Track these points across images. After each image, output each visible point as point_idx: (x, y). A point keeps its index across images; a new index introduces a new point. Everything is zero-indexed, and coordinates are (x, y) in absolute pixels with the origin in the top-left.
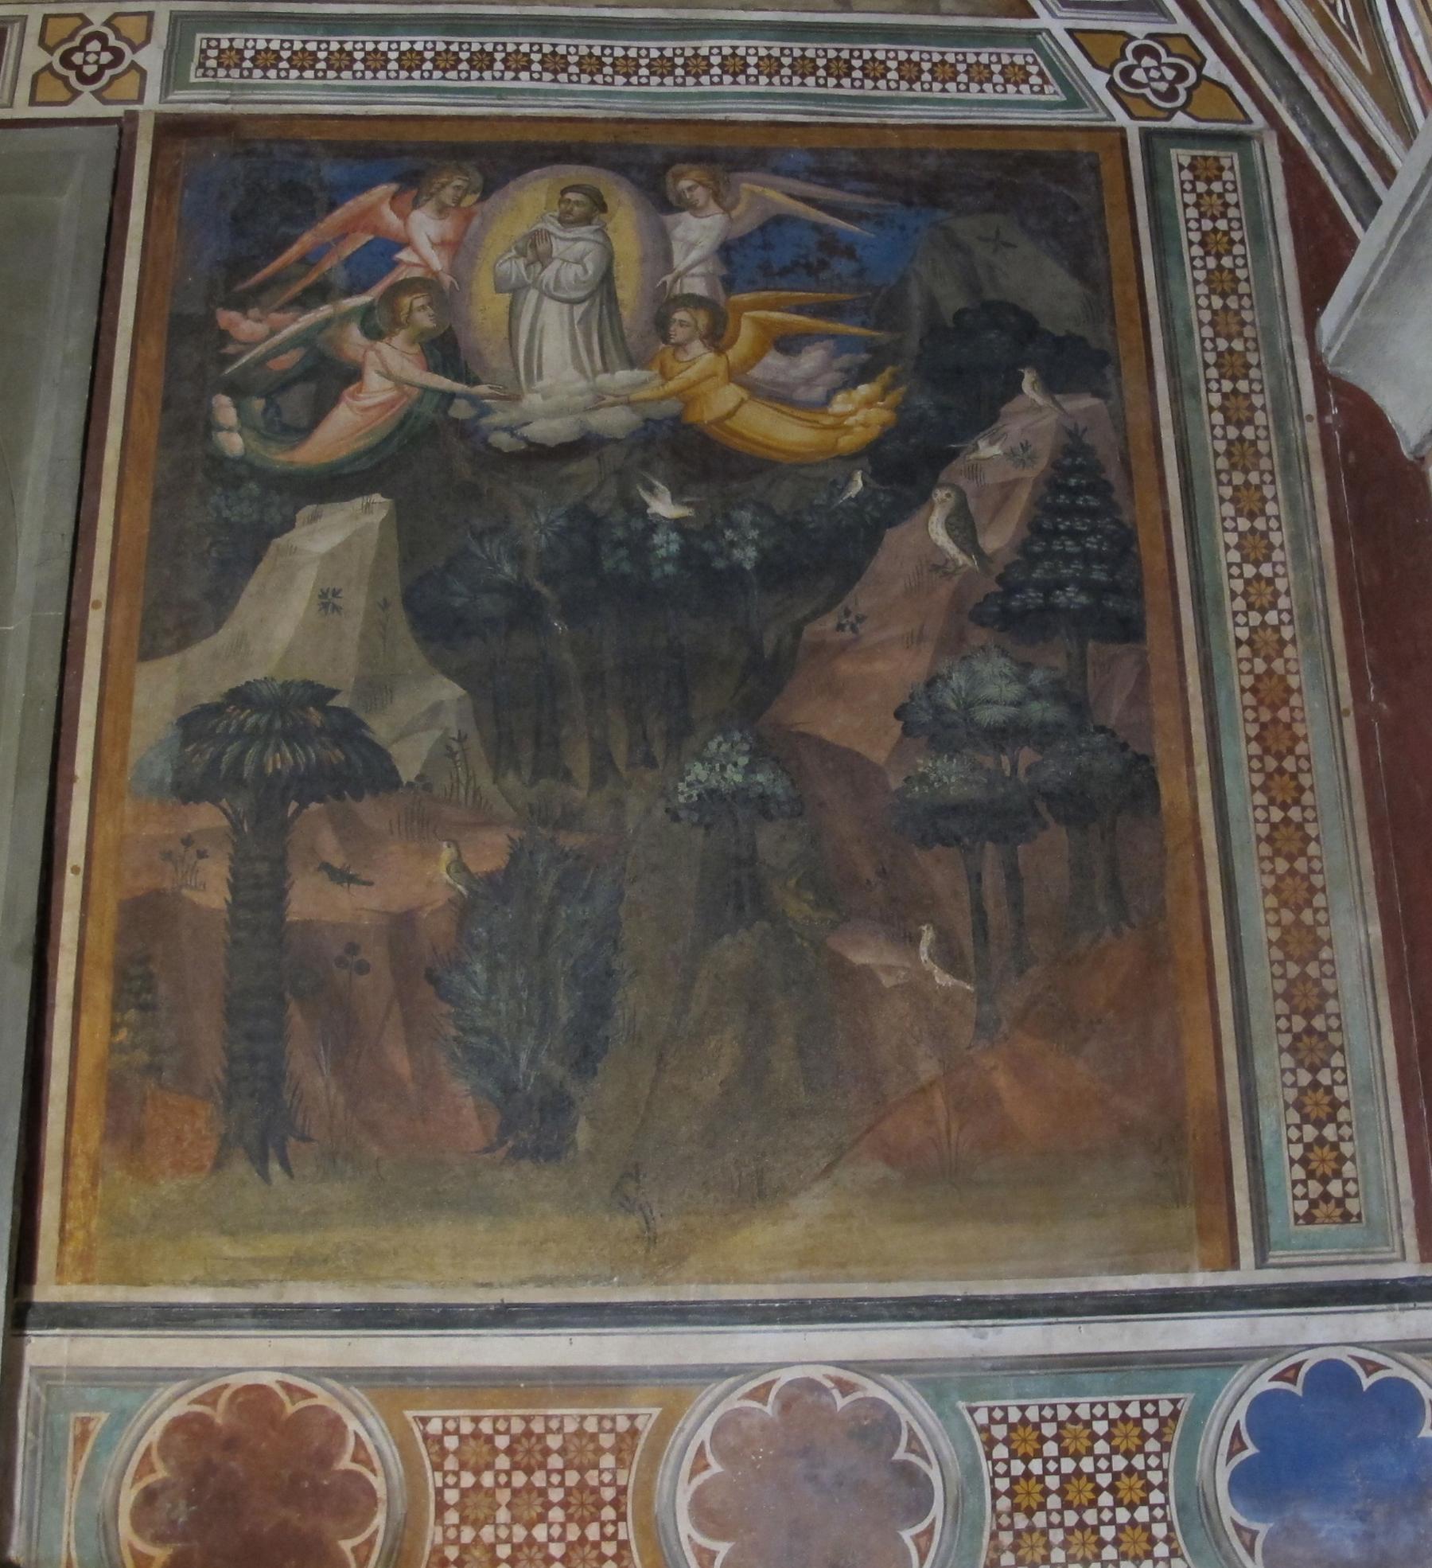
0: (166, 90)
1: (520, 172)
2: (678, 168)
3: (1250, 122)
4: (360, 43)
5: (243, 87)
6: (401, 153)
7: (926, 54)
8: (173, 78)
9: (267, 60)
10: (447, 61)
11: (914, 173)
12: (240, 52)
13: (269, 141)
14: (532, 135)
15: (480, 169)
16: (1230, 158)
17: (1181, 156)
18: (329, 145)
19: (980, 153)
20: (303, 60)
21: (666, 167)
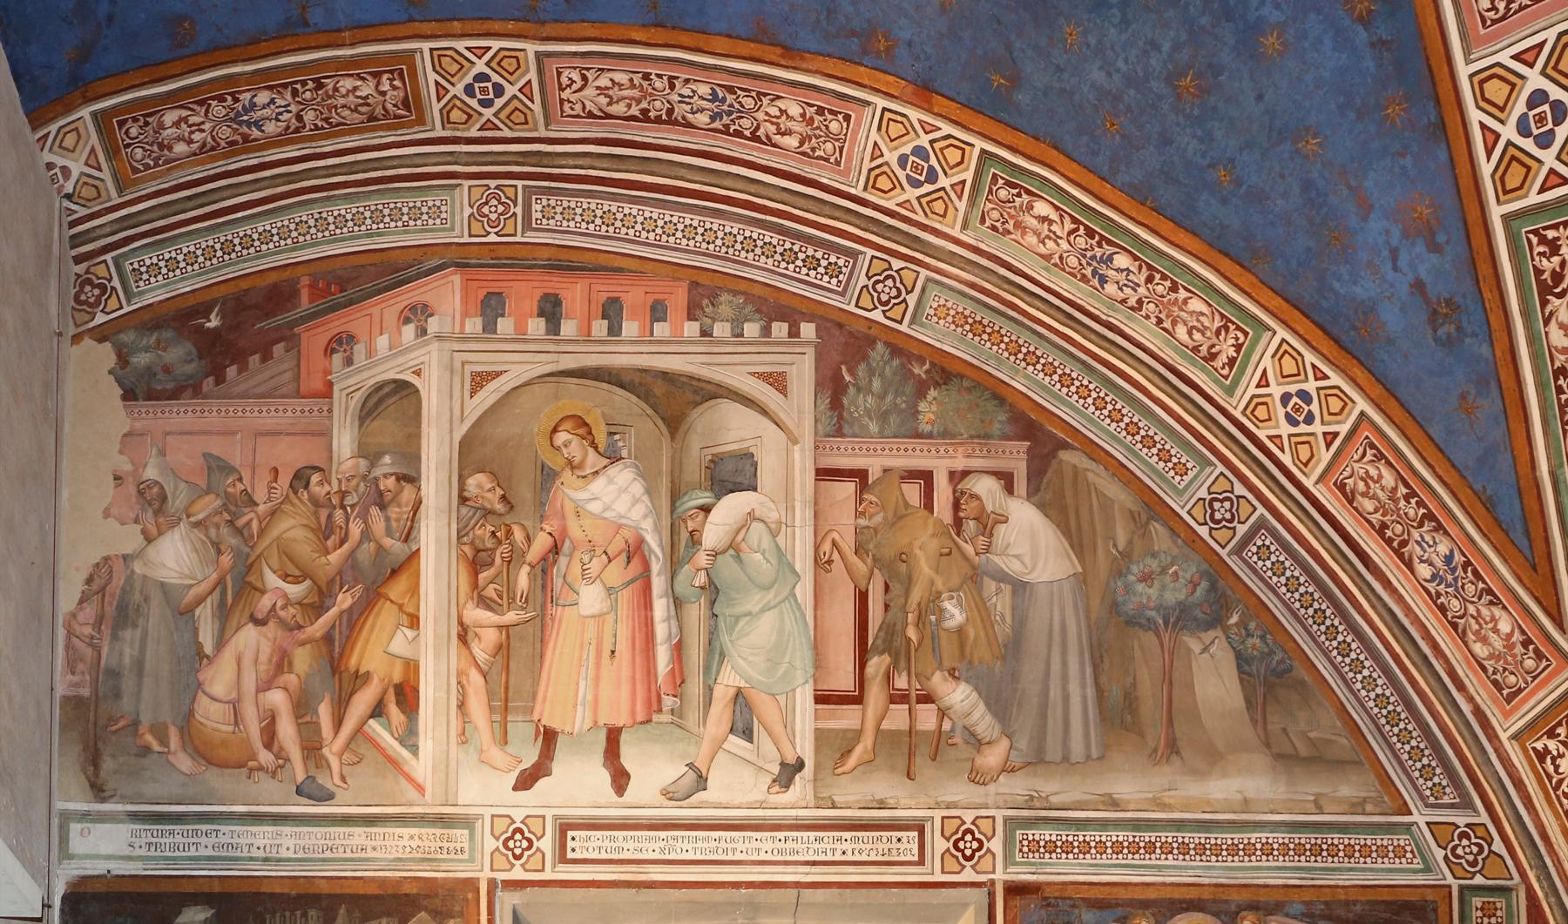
0: (1006, 867)
1: (1172, 916)
2: (1244, 913)
3: (1512, 879)
4: (1093, 836)
5: (1041, 864)
6: (1117, 905)
7: (1357, 839)
8: (1009, 860)
9: (1051, 847)
10: (1134, 848)
11: (1351, 915)
12: (1038, 842)
13: (1056, 898)
14: (1177, 894)
15: (1153, 915)
16: (1501, 902)
17: (1477, 901)
18: (1083, 899)
19: (1383, 902)
20: (1067, 848)
21: (1238, 913)
